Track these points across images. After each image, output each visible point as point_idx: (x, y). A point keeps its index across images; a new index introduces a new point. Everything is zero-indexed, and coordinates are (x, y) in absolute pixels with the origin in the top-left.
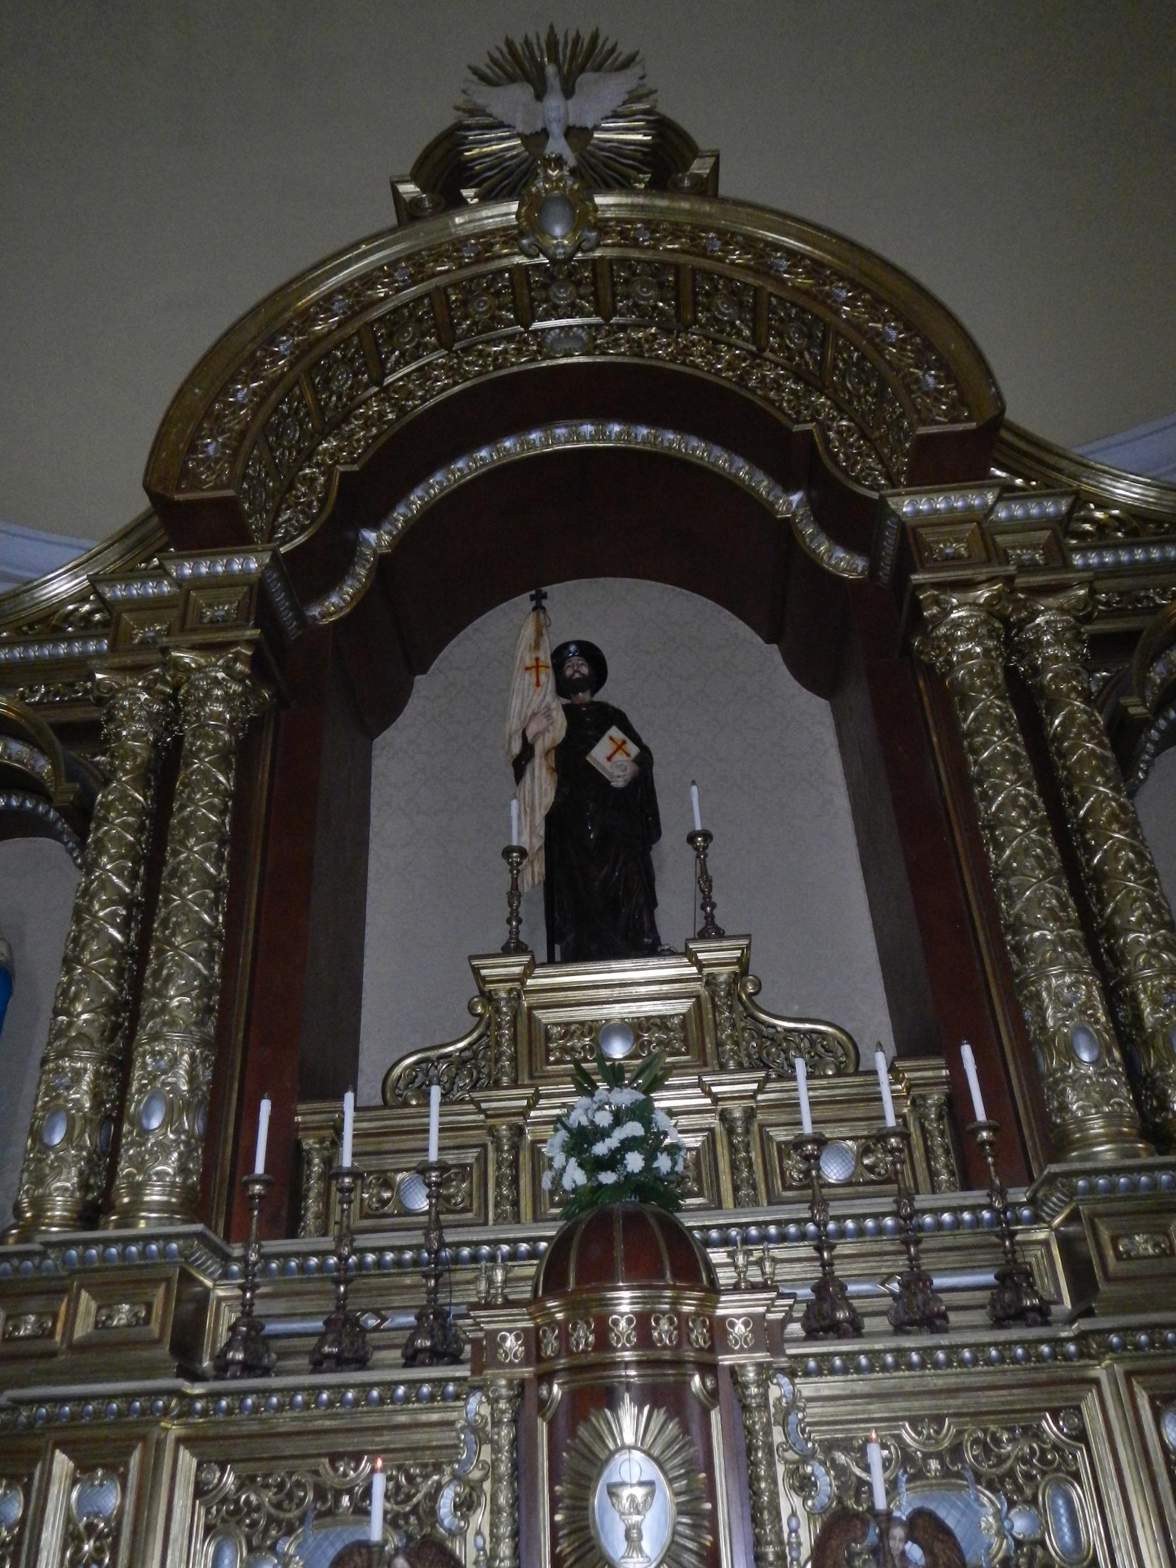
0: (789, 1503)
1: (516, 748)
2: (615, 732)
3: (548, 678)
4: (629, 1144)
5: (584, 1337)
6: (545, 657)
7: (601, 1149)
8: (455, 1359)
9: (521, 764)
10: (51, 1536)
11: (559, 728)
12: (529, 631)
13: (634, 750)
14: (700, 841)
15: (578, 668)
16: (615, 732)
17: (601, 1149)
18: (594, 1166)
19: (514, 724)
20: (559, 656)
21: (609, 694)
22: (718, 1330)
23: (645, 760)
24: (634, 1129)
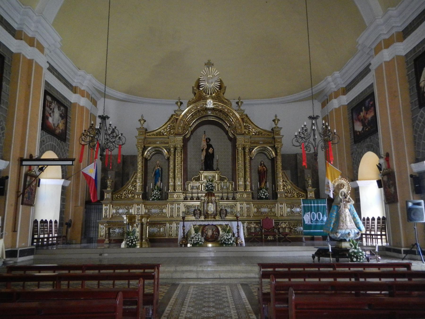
0: (219, 208)
1: (202, 149)
2: (211, 148)
3: (205, 141)
4: (211, 187)
5: (208, 199)
6: (205, 139)
7: (209, 187)
8: (199, 200)
9: (202, 150)
10: (176, 208)
11: (206, 147)
12: (204, 136)
13: (212, 150)
14: (217, 161)
15: (208, 140)
16: (211, 148)
17: (209, 187)
18: (208, 188)
19: (202, 146)
20: (206, 139)
21: (211, 143)
22: (215, 199)
23: (213, 151)
24: (211, 186)
